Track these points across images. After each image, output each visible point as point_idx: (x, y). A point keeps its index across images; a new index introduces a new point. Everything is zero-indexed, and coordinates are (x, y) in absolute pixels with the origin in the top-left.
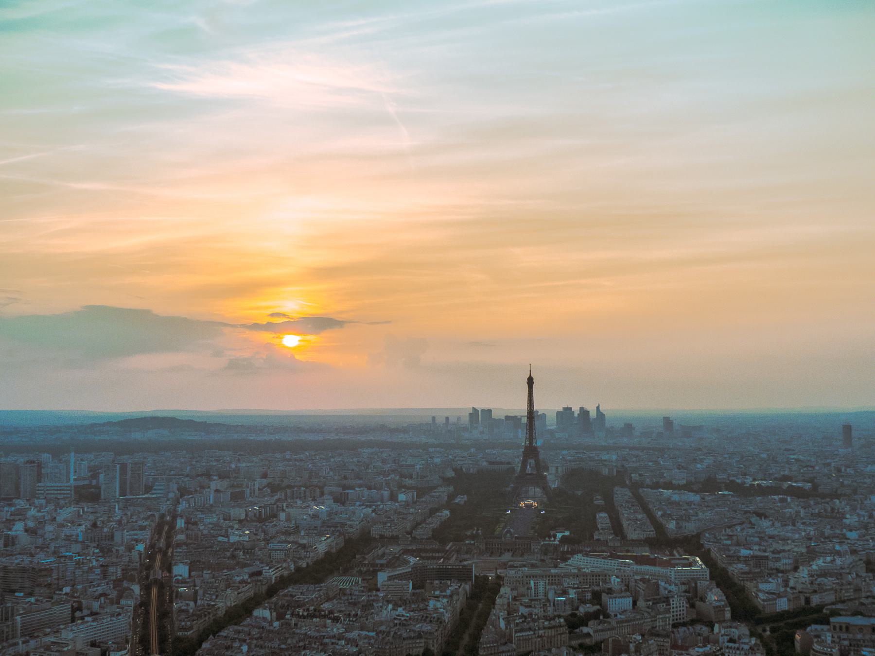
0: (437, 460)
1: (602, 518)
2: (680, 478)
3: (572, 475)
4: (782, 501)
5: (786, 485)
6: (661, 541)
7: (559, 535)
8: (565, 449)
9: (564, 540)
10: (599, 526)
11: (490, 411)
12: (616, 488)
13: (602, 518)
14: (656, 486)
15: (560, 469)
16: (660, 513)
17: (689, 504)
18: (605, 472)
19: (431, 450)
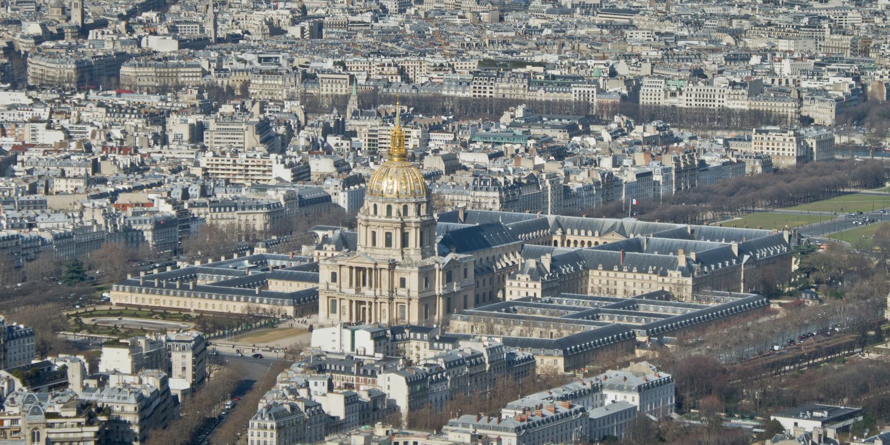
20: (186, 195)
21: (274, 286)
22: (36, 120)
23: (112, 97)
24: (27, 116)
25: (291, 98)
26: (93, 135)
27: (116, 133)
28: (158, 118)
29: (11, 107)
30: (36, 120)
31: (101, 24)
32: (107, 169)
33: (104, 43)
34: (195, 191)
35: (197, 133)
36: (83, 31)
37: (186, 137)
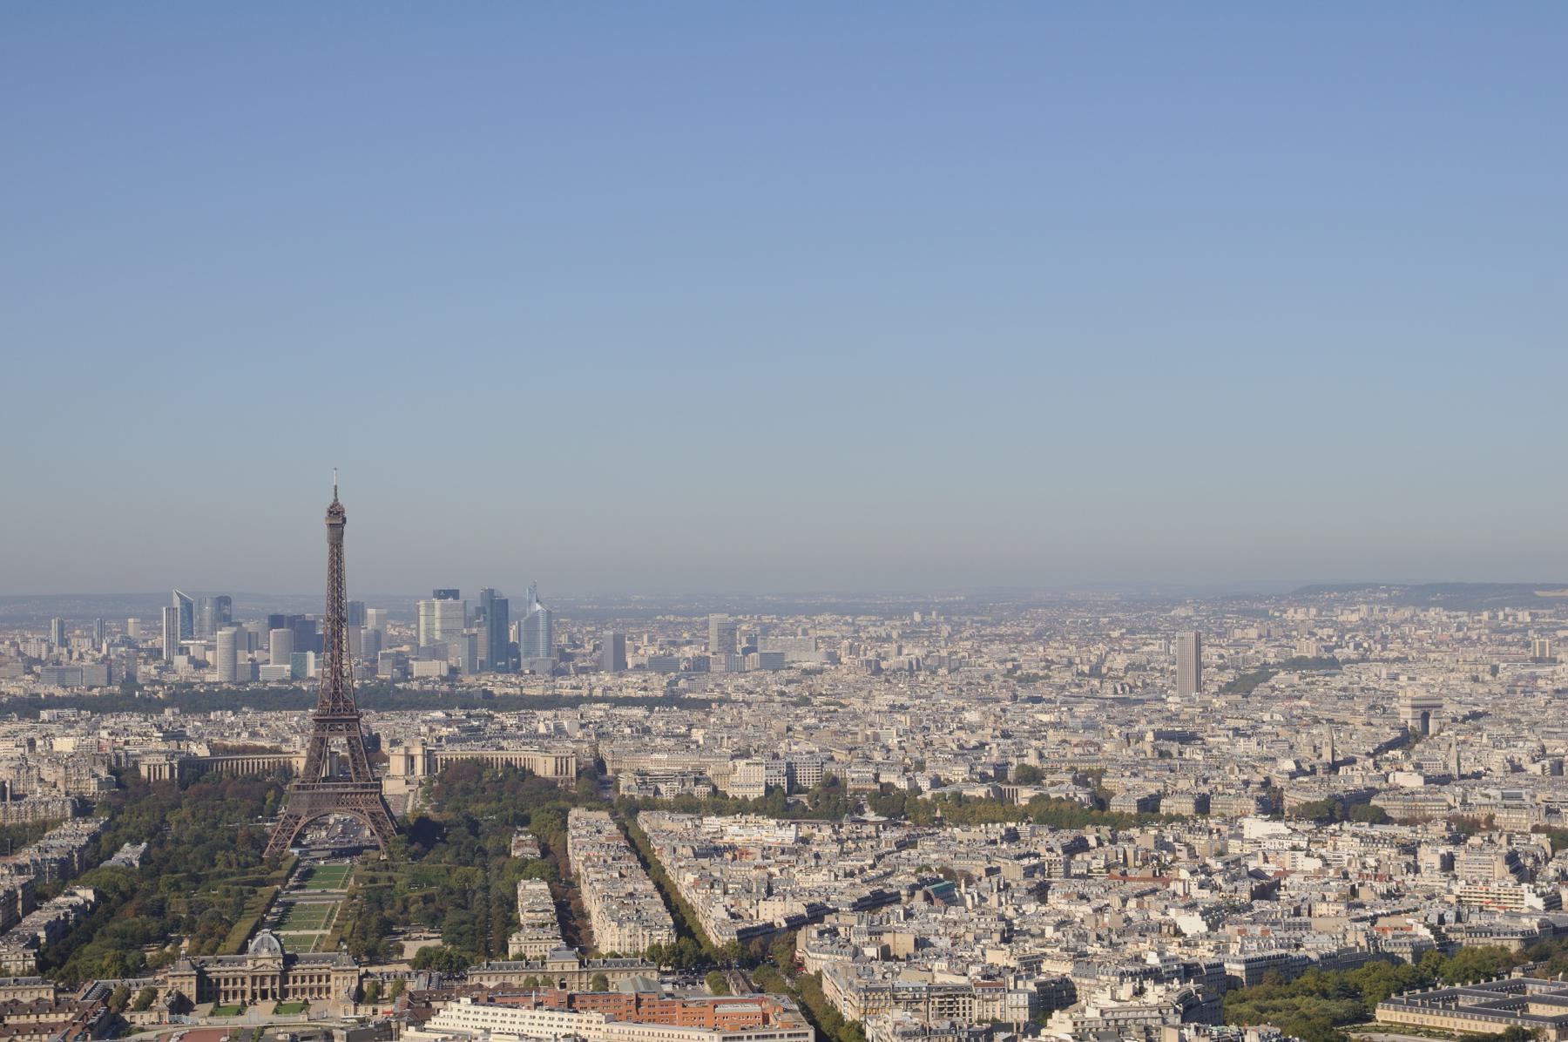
0: (64, 745)
1: (533, 894)
2: (748, 779)
3: (451, 781)
4: (1012, 836)
5: (1025, 795)
6: (689, 957)
7: (411, 950)
8: (435, 707)
9: (424, 961)
10: (524, 918)
11: (223, 601)
12: (574, 813)
13: (533, 894)
14: (687, 806)
15: (419, 762)
16: (690, 878)
17: (766, 852)
18: (544, 767)
19: (44, 715)
20: (1442, 920)
21: (1535, 1009)
22: (1294, 848)
23: (1365, 828)
24: (1288, 844)
25: (1536, 829)
26: (1350, 863)
27: (1371, 862)
28: (1410, 849)
29: (1271, 837)
30: (1294, 848)
31: (1350, 761)
32: (1365, 895)
33: (1354, 779)
34: (1450, 916)
35: (1448, 863)
36: (1334, 767)
37: (1438, 865)
